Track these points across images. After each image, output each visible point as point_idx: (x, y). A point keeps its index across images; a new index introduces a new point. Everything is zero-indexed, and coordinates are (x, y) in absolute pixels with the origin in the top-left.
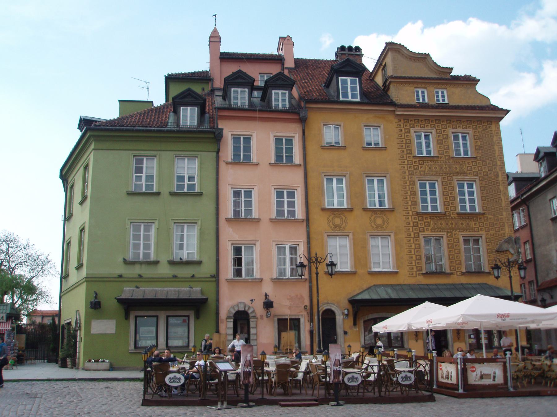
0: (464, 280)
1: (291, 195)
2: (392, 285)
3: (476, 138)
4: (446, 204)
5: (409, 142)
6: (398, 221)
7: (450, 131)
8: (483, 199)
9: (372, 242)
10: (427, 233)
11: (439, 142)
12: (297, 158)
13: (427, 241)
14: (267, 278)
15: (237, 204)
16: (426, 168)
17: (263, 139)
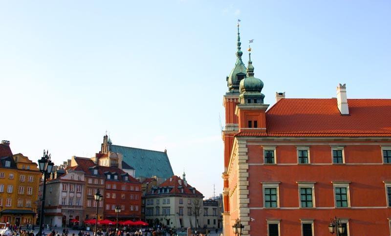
4: (24, 193)
5: (19, 178)
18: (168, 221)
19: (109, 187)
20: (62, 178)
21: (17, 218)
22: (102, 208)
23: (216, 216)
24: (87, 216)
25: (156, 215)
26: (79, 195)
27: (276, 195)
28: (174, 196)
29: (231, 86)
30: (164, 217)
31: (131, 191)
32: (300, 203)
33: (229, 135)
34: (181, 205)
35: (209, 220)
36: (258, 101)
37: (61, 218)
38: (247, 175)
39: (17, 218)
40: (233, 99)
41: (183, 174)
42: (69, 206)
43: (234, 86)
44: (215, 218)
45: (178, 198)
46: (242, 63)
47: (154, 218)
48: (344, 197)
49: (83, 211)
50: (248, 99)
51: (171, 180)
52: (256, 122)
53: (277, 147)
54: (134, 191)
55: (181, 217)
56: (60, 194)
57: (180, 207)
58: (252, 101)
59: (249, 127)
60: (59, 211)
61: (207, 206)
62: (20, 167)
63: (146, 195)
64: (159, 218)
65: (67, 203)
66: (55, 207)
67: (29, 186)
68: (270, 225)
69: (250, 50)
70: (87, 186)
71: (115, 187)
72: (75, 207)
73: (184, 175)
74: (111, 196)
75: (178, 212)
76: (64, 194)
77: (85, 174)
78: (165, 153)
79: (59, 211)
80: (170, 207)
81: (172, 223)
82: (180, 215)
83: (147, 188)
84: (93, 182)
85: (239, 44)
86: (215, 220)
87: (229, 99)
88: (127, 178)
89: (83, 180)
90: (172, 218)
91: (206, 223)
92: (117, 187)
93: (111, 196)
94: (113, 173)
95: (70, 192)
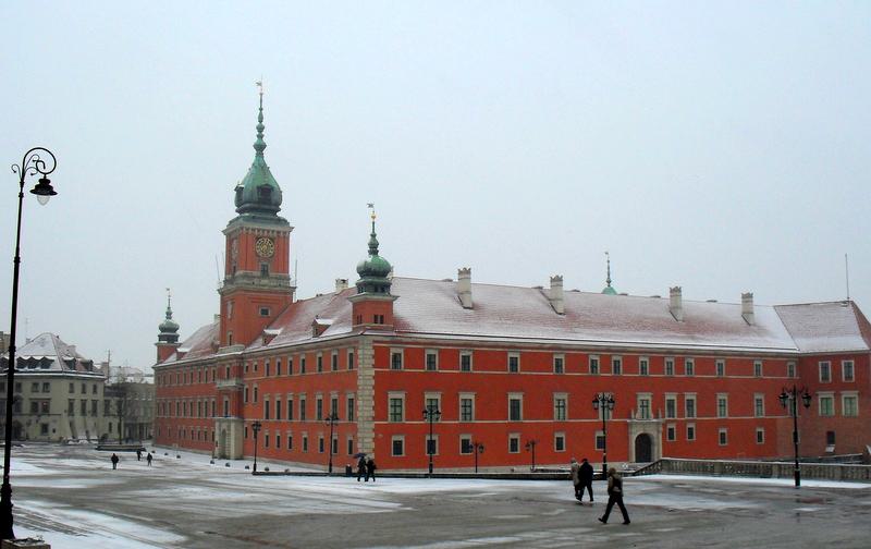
18: (45, 428)
29: (248, 205)
30: (34, 418)
35: (110, 424)
38: (373, 382)
43: (252, 205)
45: (65, 384)
48: (468, 410)
58: (380, 290)
68: (395, 442)
69: (374, 217)
75: (67, 407)
81: (54, 431)
85: (260, 129)
87: (248, 229)
91: (106, 431)
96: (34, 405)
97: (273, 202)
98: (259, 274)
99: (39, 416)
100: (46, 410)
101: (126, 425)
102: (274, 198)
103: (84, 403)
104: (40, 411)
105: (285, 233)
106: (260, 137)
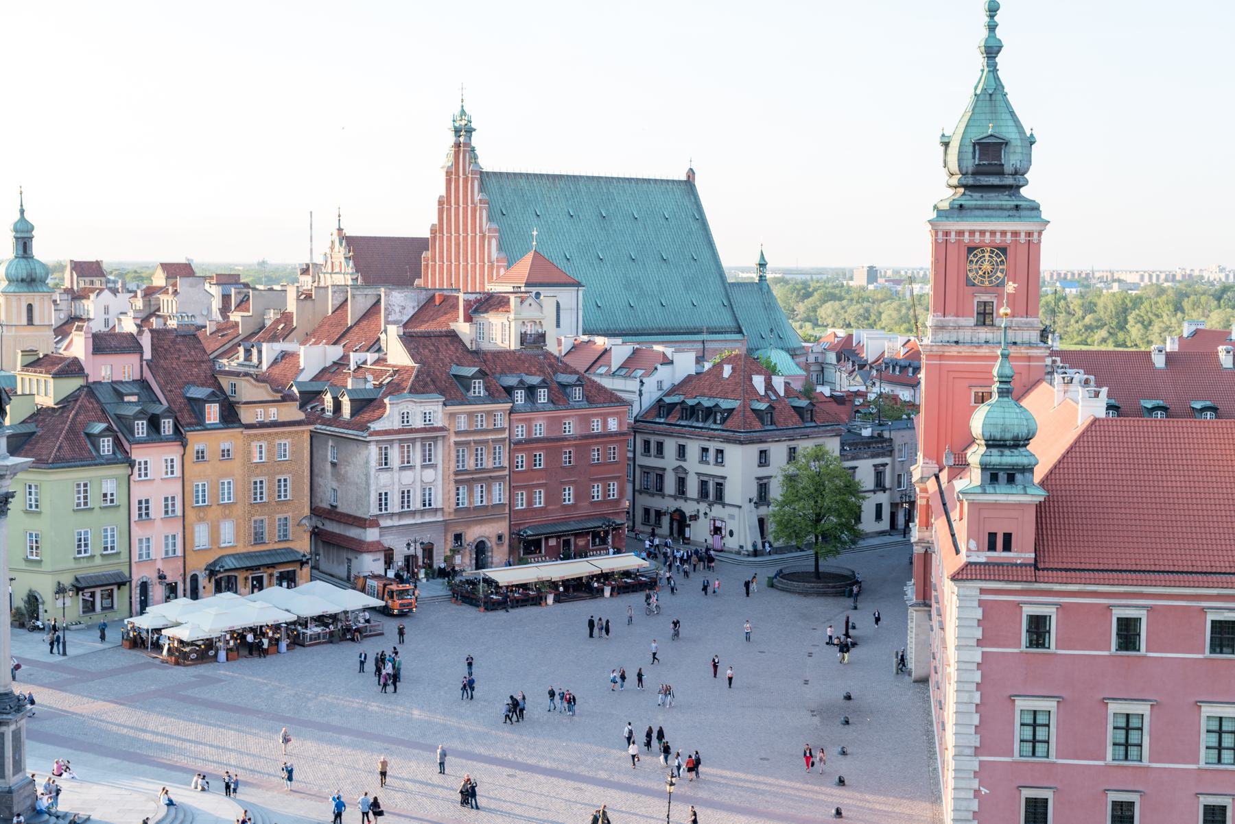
0: (276, 546)
1: (173, 498)
2: (233, 555)
3: (293, 445)
4: (269, 496)
6: (238, 511)
7: (278, 441)
8: (293, 489)
9: (222, 526)
10: (256, 518)
11: (269, 451)
12: (178, 473)
13: (255, 522)
14: (159, 558)
15: (140, 509)
16: (258, 471)
17: (157, 461)
19: (520, 433)
20: (375, 426)
21: (253, 579)
22: (504, 505)
23: (884, 490)
24: (458, 537)
25: (675, 497)
26: (429, 475)
27: (1048, 726)
28: (741, 443)
30: (703, 507)
31: (597, 436)
32: (1110, 749)
33: (941, 357)
34: (763, 472)
36: (1019, 477)
37: (381, 556)
38: (977, 677)
39: (253, 579)
40: (960, 233)
41: (757, 260)
42: (401, 515)
44: (883, 498)
45: (754, 450)
46: (999, 86)
47: (669, 504)
49: (446, 524)
50: (992, 475)
51: (727, 370)
52: (1008, 538)
53: (1060, 607)
54: (607, 435)
55: (763, 511)
56: (372, 481)
57: (758, 478)
58: (1002, 476)
59: (992, 547)
60: (371, 535)
61: (853, 459)
62: (246, 415)
63: (636, 421)
64: (689, 508)
65: (394, 505)
66: (361, 523)
67: (281, 473)
70: (453, 439)
71: (540, 428)
72: (418, 516)
73: (762, 265)
74: (533, 460)
75: (754, 494)
76: (384, 477)
77: (445, 405)
78: (689, 185)
79: (371, 535)
80: (724, 478)
81: (731, 533)
82: (757, 505)
83: (641, 395)
84: (470, 426)
86: (879, 507)
87: (947, 234)
88: (578, 393)
89: (440, 425)
90: (732, 517)
92: (548, 428)
93: (533, 460)
94: (535, 380)
95: (402, 469)
96: (704, 484)
97: (1008, 168)
98: (972, 321)
99: (710, 505)
100: (720, 497)
101: (894, 506)
102: (1011, 160)
103: (791, 479)
104: (711, 498)
105: (1029, 234)
106: (992, 28)
